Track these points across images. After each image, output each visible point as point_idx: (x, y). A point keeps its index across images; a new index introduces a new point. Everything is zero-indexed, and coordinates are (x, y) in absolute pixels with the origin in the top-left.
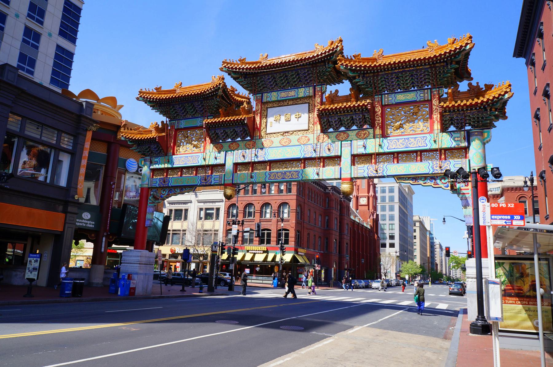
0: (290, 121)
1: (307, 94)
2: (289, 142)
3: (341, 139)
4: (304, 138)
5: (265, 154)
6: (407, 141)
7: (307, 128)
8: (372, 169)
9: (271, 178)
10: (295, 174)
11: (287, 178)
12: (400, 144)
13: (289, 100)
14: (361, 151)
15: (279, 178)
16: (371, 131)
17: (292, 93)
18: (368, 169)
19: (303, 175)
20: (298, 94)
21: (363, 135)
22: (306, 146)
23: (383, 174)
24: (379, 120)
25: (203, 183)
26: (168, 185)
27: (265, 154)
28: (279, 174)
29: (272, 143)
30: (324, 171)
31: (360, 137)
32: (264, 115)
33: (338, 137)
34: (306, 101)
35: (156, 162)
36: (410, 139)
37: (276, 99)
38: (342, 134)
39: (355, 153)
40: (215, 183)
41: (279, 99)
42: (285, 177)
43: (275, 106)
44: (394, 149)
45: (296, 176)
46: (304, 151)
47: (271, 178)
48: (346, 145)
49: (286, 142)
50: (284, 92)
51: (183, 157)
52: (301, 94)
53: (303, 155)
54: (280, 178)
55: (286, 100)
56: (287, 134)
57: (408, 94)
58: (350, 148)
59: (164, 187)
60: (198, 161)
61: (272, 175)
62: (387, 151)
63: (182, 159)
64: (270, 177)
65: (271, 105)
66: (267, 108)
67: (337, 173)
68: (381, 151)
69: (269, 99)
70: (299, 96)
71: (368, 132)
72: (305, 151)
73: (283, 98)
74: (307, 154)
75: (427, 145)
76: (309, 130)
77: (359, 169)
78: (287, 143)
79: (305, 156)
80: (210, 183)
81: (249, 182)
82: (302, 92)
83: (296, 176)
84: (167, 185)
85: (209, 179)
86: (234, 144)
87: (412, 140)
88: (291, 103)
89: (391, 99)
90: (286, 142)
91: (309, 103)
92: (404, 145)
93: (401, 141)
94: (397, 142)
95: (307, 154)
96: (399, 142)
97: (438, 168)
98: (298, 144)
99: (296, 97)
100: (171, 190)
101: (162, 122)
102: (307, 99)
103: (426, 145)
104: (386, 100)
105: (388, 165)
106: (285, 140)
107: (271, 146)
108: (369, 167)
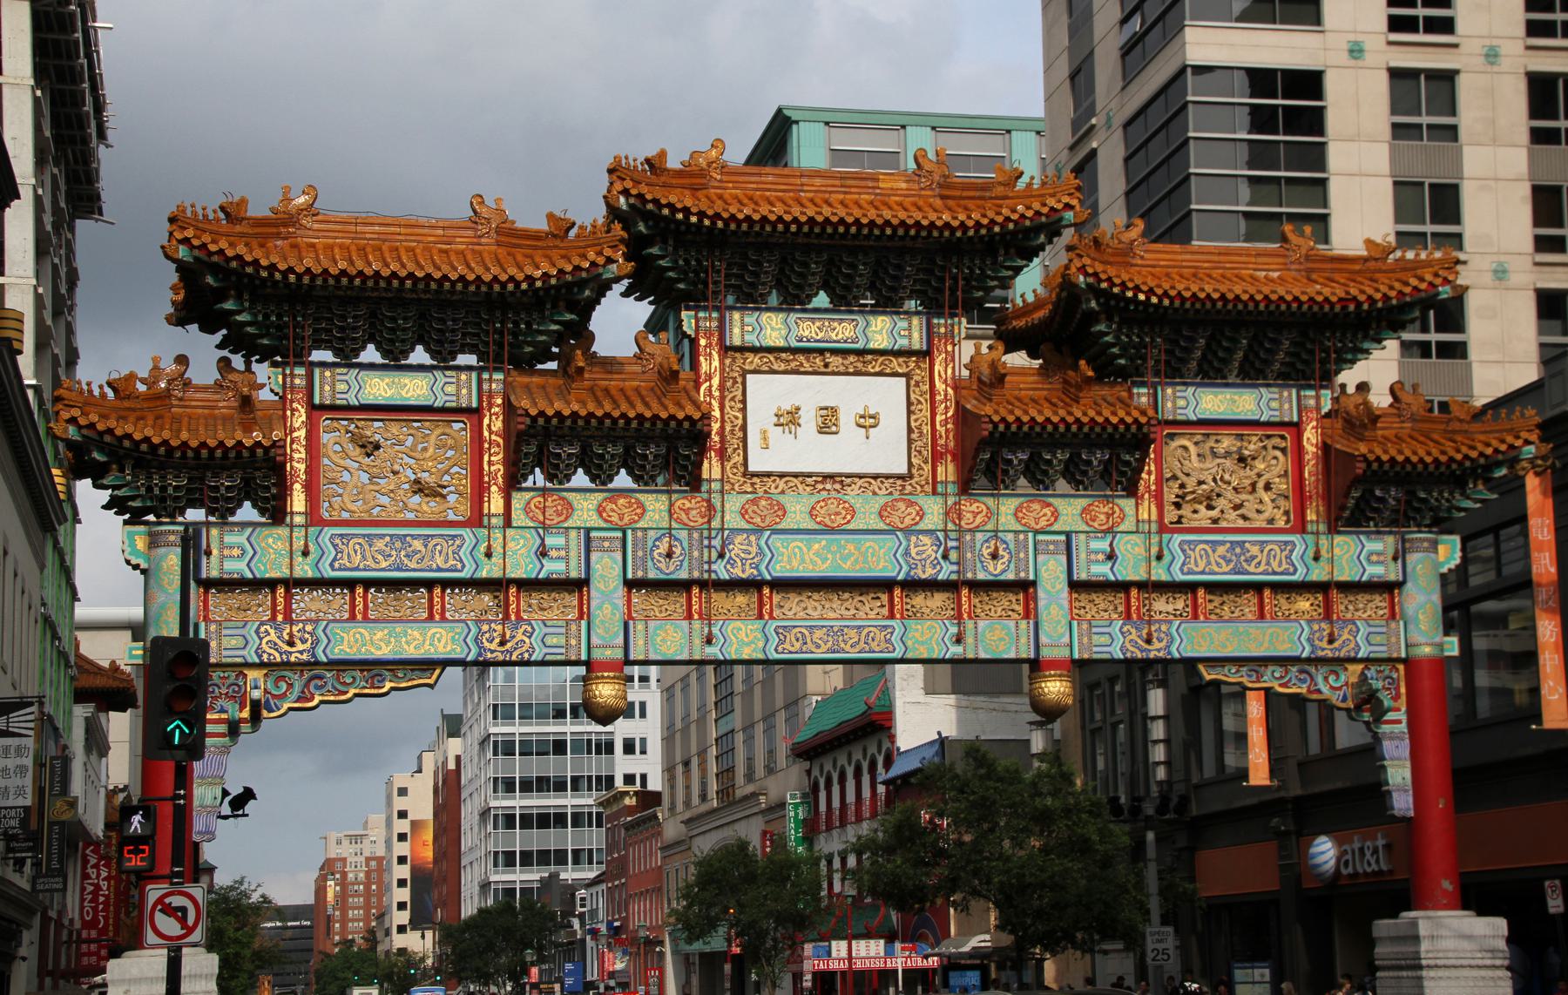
0: (836, 433)
1: (903, 343)
2: (849, 517)
3: (1033, 524)
4: (902, 505)
5: (761, 553)
6: (1238, 550)
7: (903, 470)
8: (1134, 636)
9: (787, 646)
10: (880, 636)
11: (847, 648)
12: (1221, 561)
13: (834, 352)
14: (1101, 571)
15: (818, 647)
16: (1128, 504)
17: (843, 330)
18: (1122, 633)
19: (909, 643)
20: (870, 335)
21: (1103, 517)
22: (913, 538)
23: (1169, 653)
24: (1149, 473)
25: (492, 652)
26: (314, 655)
27: (761, 553)
28: (818, 634)
29: (780, 513)
30: (980, 630)
31: (1096, 524)
32: (733, 399)
33: (1020, 515)
34: (896, 364)
35: (236, 552)
36: (1247, 545)
37: (781, 343)
38: (1036, 506)
39: (1084, 576)
40: (549, 658)
41: (794, 344)
42: (842, 645)
43: (775, 367)
44: (1202, 573)
45: (883, 645)
46: (907, 553)
47: (787, 646)
48: (1051, 547)
49: (837, 514)
50: (813, 320)
51: (382, 536)
52: (878, 337)
53: (905, 568)
54: (824, 648)
55: (821, 352)
56: (828, 486)
57: (1235, 394)
58: (1064, 559)
59: (287, 665)
60: (461, 561)
61: (791, 637)
62: (1180, 577)
63: (380, 544)
64: (781, 642)
65: (754, 360)
66: (744, 373)
67: (1023, 640)
68: (1160, 574)
69: (751, 339)
70: (871, 346)
71: (1121, 510)
72: (913, 555)
73: (808, 341)
74: (919, 567)
75: (1296, 570)
76: (911, 476)
77: (1094, 630)
78: (840, 520)
79: (912, 573)
80: (526, 655)
81: (697, 657)
82: (881, 331)
83: (883, 645)
84: (305, 657)
85: (519, 637)
86: (622, 501)
87: (1255, 550)
88: (835, 361)
89: (1181, 403)
90: (837, 514)
91: (908, 376)
92: (1231, 566)
93: (1221, 550)
94: (1210, 551)
95: (919, 567)
96: (1217, 554)
97: (1324, 644)
98: (882, 526)
99: (860, 345)
100: (320, 678)
101: (225, 364)
102: (901, 360)
103: (1291, 570)
104: (1169, 405)
105: (1183, 626)
106: (833, 507)
107: (779, 527)
108: (1125, 629)
